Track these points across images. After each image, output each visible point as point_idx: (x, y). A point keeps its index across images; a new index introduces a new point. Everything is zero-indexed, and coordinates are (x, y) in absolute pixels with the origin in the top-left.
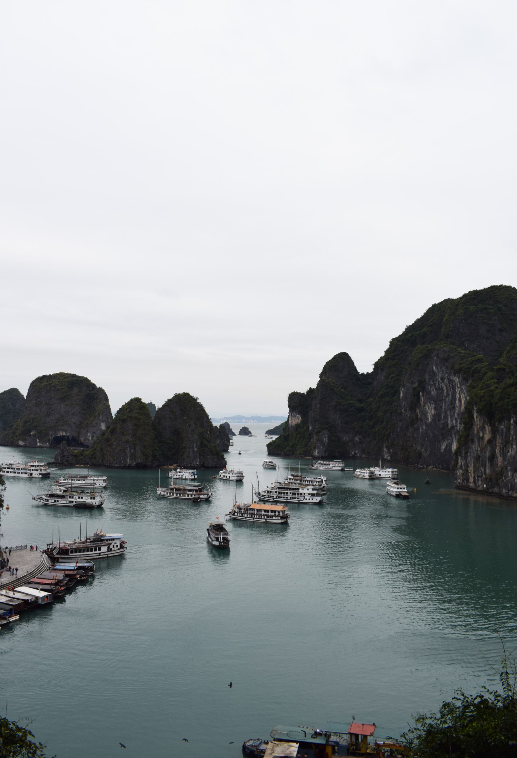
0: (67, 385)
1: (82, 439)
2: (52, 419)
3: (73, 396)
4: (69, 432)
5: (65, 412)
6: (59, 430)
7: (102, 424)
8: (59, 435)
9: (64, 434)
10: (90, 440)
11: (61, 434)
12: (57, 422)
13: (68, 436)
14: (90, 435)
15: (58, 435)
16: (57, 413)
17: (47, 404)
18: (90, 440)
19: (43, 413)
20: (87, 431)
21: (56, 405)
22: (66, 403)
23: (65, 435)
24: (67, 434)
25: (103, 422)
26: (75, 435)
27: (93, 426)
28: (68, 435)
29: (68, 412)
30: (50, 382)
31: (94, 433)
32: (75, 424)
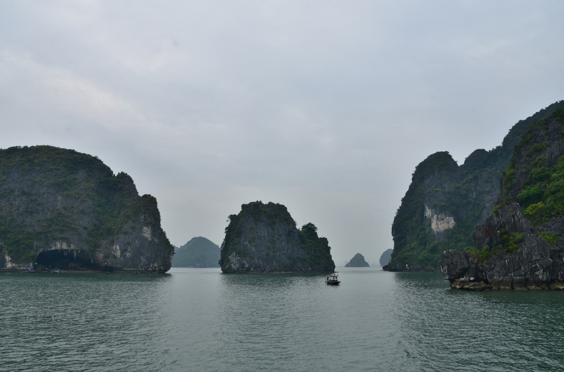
0: (65, 164)
1: (100, 256)
2: (39, 220)
3: (80, 182)
4: (74, 243)
5: (65, 208)
6: (55, 239)
7: (145, 228)
8: (54, 249)
9: (65, 246)
10: (119, 257)
11: (58, 246)
12: (50, 226)
13: (72, 250)
14: (118, 248)
15: (51, 247)
16: (49, 210)
17: (24, 193)
18: (119, 257)
19: (18, 210)
20: (112, 243)
21: (45, 196)
22: (65, 193)
23: (66, 248)
24: (70, 246)
25: (147, 225)
26: (86, 248)
27: (126, 233)
28: (72, 247)
29: (72, 207)
30: (30, 157)
31: (129, 244)
32: (85, 228)
